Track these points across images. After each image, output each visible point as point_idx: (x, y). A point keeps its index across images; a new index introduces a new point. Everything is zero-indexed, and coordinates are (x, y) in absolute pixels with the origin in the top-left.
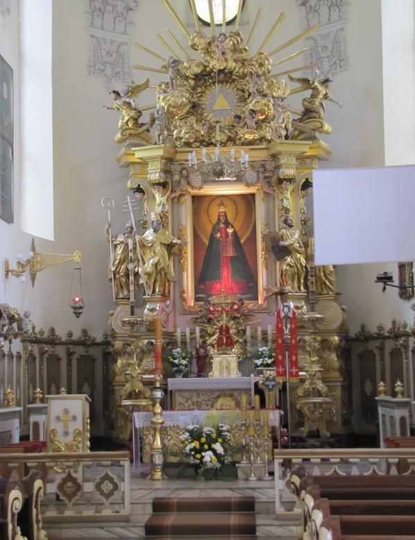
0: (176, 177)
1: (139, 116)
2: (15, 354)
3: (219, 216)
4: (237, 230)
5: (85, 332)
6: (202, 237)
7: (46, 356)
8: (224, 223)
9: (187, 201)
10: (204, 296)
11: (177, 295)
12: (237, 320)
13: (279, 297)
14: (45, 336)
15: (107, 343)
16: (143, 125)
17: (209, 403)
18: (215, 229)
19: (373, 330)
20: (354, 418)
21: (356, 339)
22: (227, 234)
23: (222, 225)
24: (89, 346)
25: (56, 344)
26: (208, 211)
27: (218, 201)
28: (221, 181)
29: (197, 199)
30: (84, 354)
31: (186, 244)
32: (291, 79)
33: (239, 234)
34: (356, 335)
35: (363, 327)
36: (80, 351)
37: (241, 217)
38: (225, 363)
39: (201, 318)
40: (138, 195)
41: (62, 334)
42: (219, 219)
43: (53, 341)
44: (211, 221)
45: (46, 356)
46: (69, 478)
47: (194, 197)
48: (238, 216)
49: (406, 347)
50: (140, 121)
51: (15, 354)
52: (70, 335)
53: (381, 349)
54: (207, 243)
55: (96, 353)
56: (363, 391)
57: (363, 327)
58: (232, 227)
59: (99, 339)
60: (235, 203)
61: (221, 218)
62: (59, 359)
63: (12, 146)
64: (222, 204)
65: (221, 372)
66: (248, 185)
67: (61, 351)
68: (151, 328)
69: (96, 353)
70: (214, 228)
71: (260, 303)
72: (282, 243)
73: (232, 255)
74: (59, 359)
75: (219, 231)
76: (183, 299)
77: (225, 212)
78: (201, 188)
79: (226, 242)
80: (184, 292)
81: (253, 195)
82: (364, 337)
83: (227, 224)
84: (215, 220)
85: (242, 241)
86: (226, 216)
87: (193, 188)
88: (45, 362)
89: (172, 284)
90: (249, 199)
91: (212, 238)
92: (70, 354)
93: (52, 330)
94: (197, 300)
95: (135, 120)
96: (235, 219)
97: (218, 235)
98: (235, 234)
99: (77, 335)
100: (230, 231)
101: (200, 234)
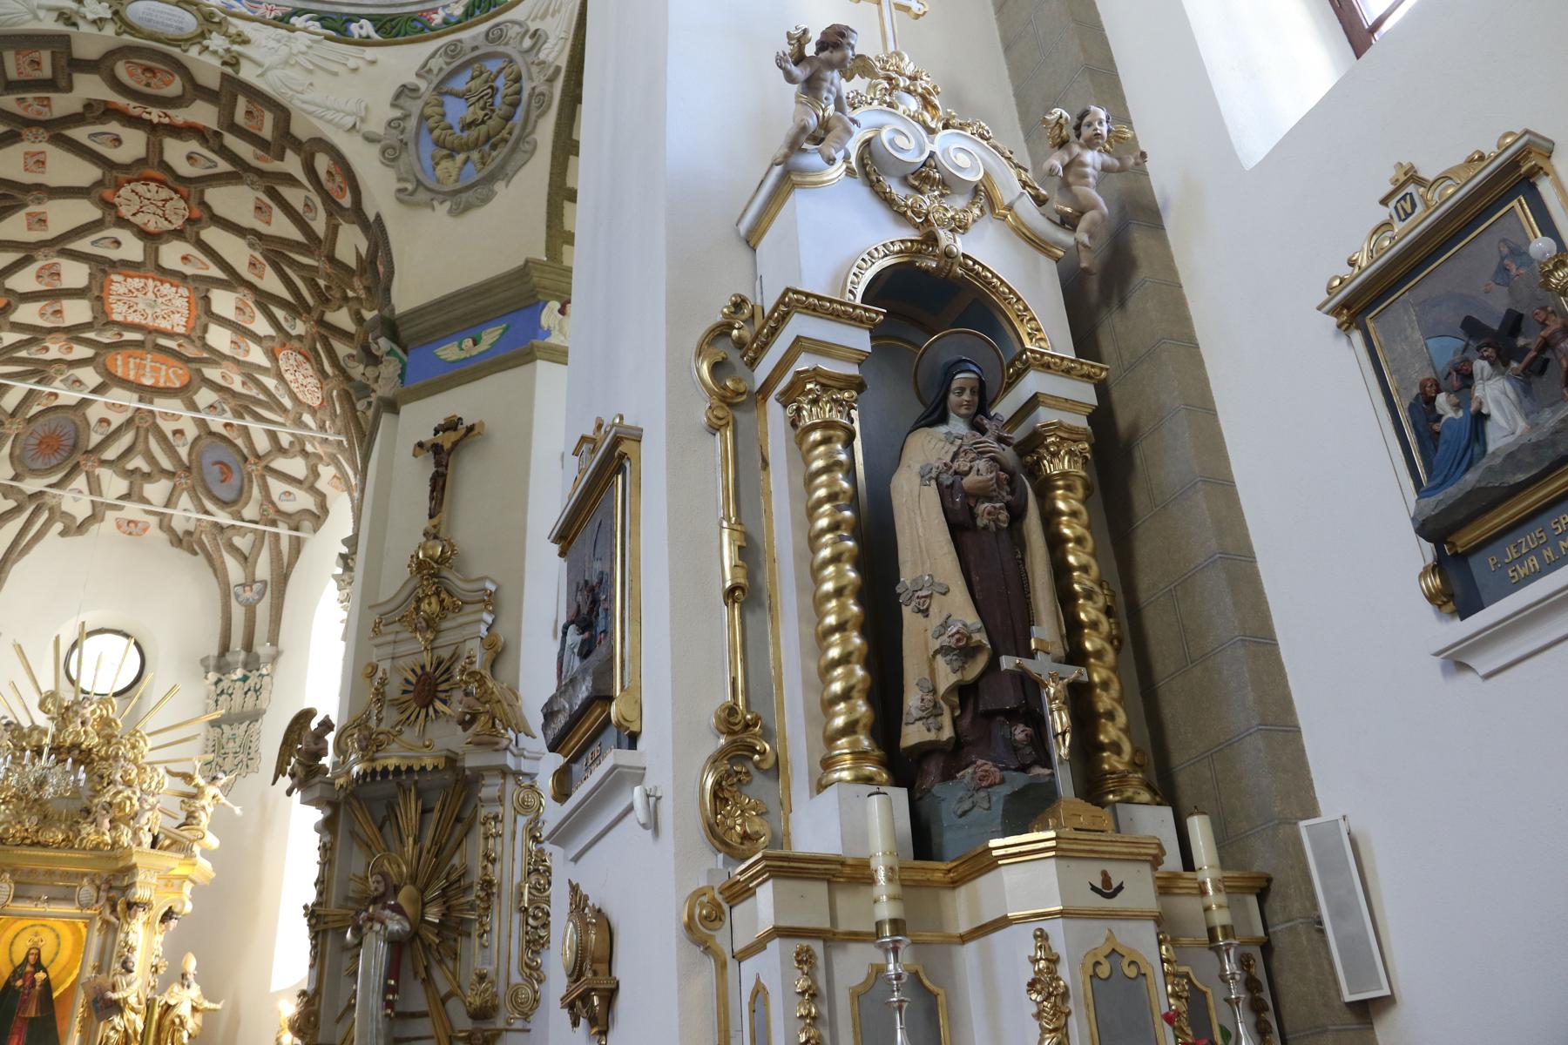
22: (34, 981)
23: (29, 968)
32: (169, 772)
33: (53, 984)
42: (26, 959)
58: (45, 971)
70: (14, 972)
72: (110, 995)
73: (33, 1014)
83: (38, 966)
85: (55, 995)
86: (39, 954)
97: (19, 983)
98: (47, 982)
100: (40, 976)
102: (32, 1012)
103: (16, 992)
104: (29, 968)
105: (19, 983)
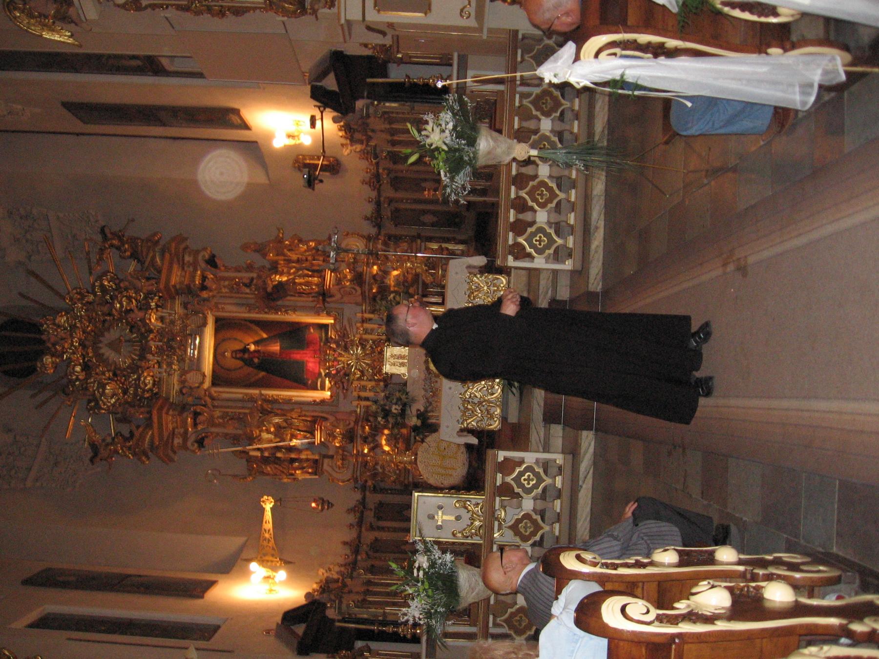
0: (190, 400)
1: (121, 435)
2: (366, 588)
3: (236, 358)
4: (251, 340)
5: (349, 511)
6: (257, 377)
7: (370, 553)
9: (214, 390)
10: (319, 380)
11: (317, 408)
12: (349, 345)
13: (328, 300)
14: (348, 552)
15: (364, 488)
16: (131, 432)
17: (433, 379)
18: (248, 362)
19: (369, 209)
20: (459, 237)
21: (379, 226)
22: (255, 351)
23: (246, 356)
24: (364, 507)
25: (360, 542)
27: (219, 357)
28: (199, 352)
29: (218, 379)
30: (373, 513)
31: (261, 395)
33: (256, 339)
34: (374, 226)
35: (367, 218)
36: (369, 516)
37: (239, 335)
38: (392, 360)
39: (343, 383)
40: (206, 442)
41: (350, 535)
43: (355, 547)
45: (370, 553)
46: (514, 528)
47: (214, 384)
48: (238, 338)
49: (390, 171)
50: (127, 435)
51: (366, 588)
52: (351, 526)
53: (391, 201)
55: (373, 499)
56: (433, 225)
57: (367, 218)
59: (358, 496)
60: (224, 340)
61: (238, 356)
62: (376, 539)
63: (130, 576)
64: (223, 354)
65: (402, 365)
66: (205, 324)
67: (369, 537)
68: (350, 436)
69: (373, 499)
71: (332, 321)
74: (376, 539)
76: (323, 402)
77: (232, 352)
78: (204, 375)
80: (315, 401)
81: (217, 320)
82: (376, 220)
84: (239, 363)
85: (265, 336)
86: (236, 351)
87: (202, 383)
88: (378, 555)
89: (304, 413)
90: (222, 325)
91: (260, 367)
92: (372, 528)
93: (345, 543)
94: (323, 388)
95: (127, 439)
96: (241, 341)
97: (256, 360)
98: (256, 343)
99: (352, 519)
101: (253, 380)
104: (246, 356)
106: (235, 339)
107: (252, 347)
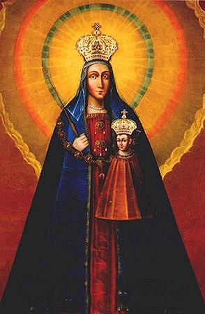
4: (148, 127)
8: (99, 101)
22: (112, 136)
23: (94, 109)
26: (45, 52)
33: (155, 143)
42: (85, 84)
44: (54, 92)
54: (38, 168)
58: (132, 116)
61: (94, 83)
70: (64, 117)
75: (84, 126)
79: (106, 167)
83: (113, 103)
85: (165, 170)
86: (110, 76)
97: (80, 143)
98: (139, 137)
100: (123, 127)
102: (121, 208)
103: (78, 162)
104: (94, 109)
105: (80, 143)
106: (150, 73)
107: (123, 127)
